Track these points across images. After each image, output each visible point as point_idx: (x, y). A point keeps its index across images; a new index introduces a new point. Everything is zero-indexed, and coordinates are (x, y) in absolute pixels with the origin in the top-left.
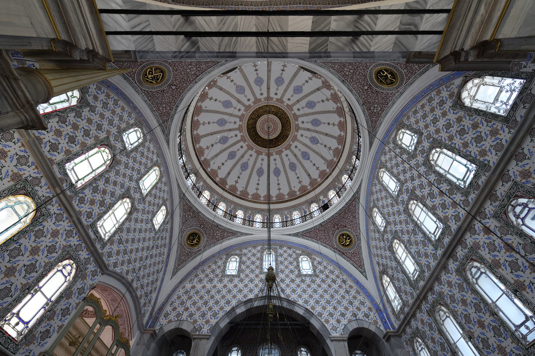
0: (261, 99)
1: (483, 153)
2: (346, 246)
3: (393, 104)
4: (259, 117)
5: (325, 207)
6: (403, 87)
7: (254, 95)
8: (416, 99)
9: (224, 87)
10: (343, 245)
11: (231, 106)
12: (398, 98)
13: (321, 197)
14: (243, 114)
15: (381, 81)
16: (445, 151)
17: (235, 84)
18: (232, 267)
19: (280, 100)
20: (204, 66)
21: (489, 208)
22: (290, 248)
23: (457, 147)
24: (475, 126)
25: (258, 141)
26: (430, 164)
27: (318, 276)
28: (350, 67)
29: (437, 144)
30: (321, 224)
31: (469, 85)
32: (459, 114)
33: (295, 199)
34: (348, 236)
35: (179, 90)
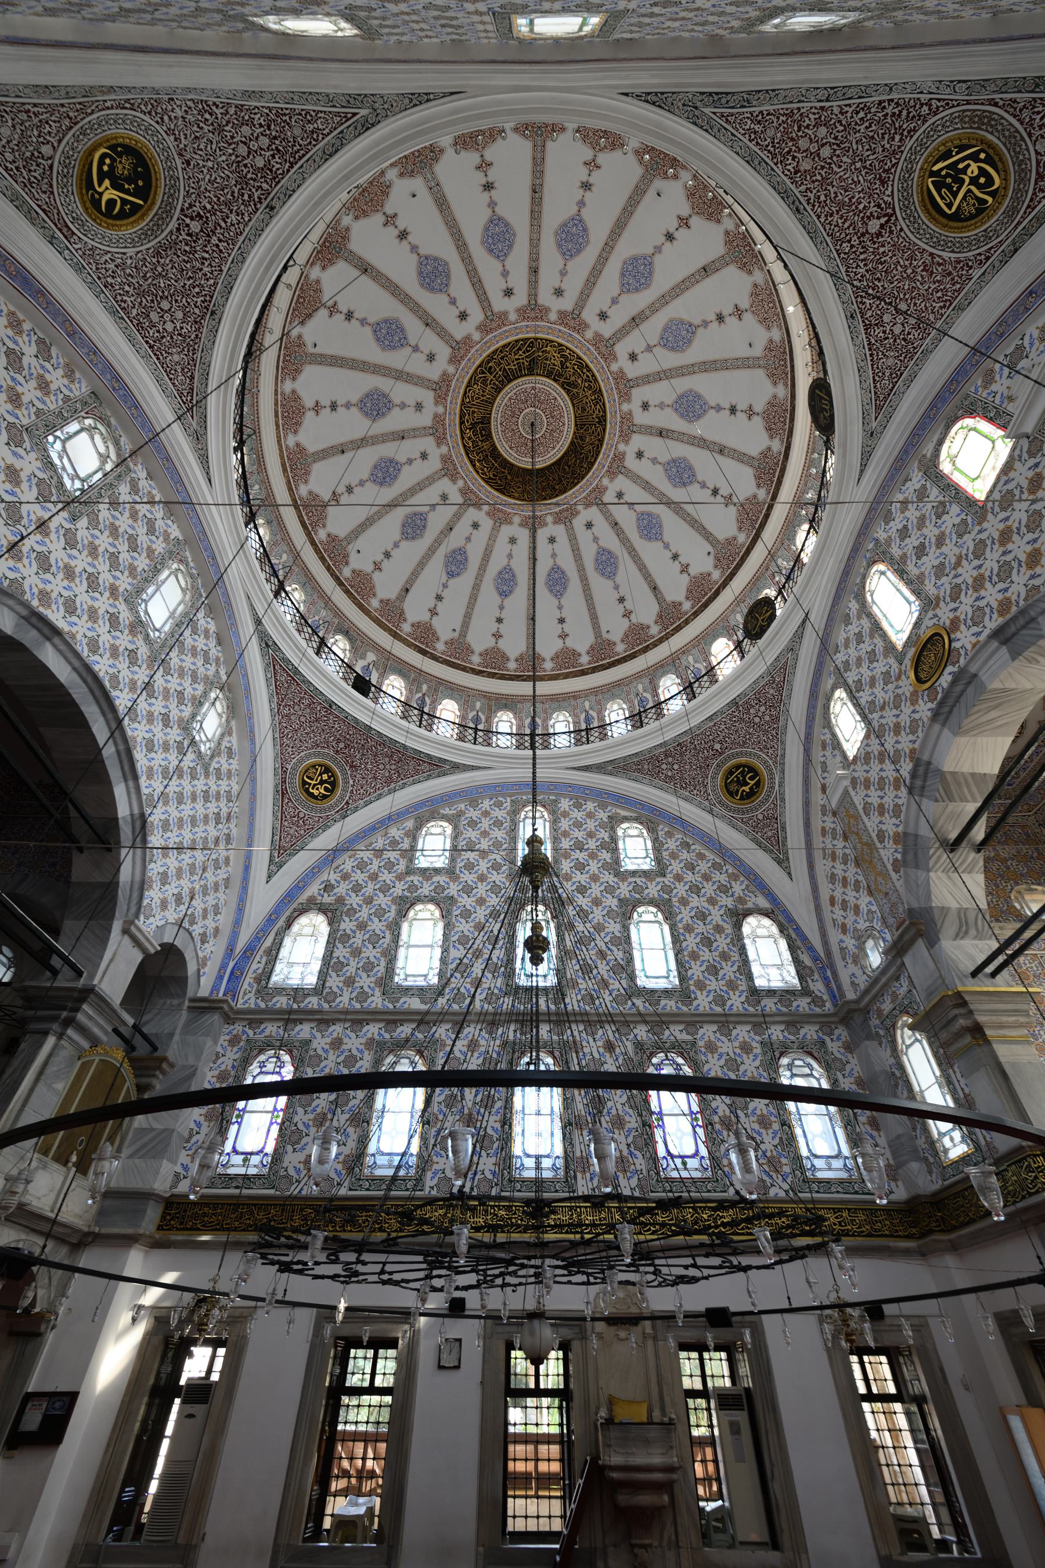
0: (629, 400)
1: (701, 985)
2: (307, 791)
3: (686, 799)
4: (568, 386)
5: (362, 685)
6: (725, 812)
7: (647, 379)
9: (709, 283)
10: (304, 783)
11: (626, 288)
12: (699, 805)
14: (587, 326)
15: (731, 773)
16: (666, 928)
17: (705, 324)
18: (83, 454)
19: (618, 467)
20: (890, 362)
22: (219, 643)
23: (684, 944)
24: (725, 956)
25: (485, 381)
26: (631, 914)
27: (207, 775)
28: (767, 718)
30: (331, 704)
31: (767, 922)
32: (725, 926)
33: (328, 568)
34: (334, 784)
35: (855, 241)
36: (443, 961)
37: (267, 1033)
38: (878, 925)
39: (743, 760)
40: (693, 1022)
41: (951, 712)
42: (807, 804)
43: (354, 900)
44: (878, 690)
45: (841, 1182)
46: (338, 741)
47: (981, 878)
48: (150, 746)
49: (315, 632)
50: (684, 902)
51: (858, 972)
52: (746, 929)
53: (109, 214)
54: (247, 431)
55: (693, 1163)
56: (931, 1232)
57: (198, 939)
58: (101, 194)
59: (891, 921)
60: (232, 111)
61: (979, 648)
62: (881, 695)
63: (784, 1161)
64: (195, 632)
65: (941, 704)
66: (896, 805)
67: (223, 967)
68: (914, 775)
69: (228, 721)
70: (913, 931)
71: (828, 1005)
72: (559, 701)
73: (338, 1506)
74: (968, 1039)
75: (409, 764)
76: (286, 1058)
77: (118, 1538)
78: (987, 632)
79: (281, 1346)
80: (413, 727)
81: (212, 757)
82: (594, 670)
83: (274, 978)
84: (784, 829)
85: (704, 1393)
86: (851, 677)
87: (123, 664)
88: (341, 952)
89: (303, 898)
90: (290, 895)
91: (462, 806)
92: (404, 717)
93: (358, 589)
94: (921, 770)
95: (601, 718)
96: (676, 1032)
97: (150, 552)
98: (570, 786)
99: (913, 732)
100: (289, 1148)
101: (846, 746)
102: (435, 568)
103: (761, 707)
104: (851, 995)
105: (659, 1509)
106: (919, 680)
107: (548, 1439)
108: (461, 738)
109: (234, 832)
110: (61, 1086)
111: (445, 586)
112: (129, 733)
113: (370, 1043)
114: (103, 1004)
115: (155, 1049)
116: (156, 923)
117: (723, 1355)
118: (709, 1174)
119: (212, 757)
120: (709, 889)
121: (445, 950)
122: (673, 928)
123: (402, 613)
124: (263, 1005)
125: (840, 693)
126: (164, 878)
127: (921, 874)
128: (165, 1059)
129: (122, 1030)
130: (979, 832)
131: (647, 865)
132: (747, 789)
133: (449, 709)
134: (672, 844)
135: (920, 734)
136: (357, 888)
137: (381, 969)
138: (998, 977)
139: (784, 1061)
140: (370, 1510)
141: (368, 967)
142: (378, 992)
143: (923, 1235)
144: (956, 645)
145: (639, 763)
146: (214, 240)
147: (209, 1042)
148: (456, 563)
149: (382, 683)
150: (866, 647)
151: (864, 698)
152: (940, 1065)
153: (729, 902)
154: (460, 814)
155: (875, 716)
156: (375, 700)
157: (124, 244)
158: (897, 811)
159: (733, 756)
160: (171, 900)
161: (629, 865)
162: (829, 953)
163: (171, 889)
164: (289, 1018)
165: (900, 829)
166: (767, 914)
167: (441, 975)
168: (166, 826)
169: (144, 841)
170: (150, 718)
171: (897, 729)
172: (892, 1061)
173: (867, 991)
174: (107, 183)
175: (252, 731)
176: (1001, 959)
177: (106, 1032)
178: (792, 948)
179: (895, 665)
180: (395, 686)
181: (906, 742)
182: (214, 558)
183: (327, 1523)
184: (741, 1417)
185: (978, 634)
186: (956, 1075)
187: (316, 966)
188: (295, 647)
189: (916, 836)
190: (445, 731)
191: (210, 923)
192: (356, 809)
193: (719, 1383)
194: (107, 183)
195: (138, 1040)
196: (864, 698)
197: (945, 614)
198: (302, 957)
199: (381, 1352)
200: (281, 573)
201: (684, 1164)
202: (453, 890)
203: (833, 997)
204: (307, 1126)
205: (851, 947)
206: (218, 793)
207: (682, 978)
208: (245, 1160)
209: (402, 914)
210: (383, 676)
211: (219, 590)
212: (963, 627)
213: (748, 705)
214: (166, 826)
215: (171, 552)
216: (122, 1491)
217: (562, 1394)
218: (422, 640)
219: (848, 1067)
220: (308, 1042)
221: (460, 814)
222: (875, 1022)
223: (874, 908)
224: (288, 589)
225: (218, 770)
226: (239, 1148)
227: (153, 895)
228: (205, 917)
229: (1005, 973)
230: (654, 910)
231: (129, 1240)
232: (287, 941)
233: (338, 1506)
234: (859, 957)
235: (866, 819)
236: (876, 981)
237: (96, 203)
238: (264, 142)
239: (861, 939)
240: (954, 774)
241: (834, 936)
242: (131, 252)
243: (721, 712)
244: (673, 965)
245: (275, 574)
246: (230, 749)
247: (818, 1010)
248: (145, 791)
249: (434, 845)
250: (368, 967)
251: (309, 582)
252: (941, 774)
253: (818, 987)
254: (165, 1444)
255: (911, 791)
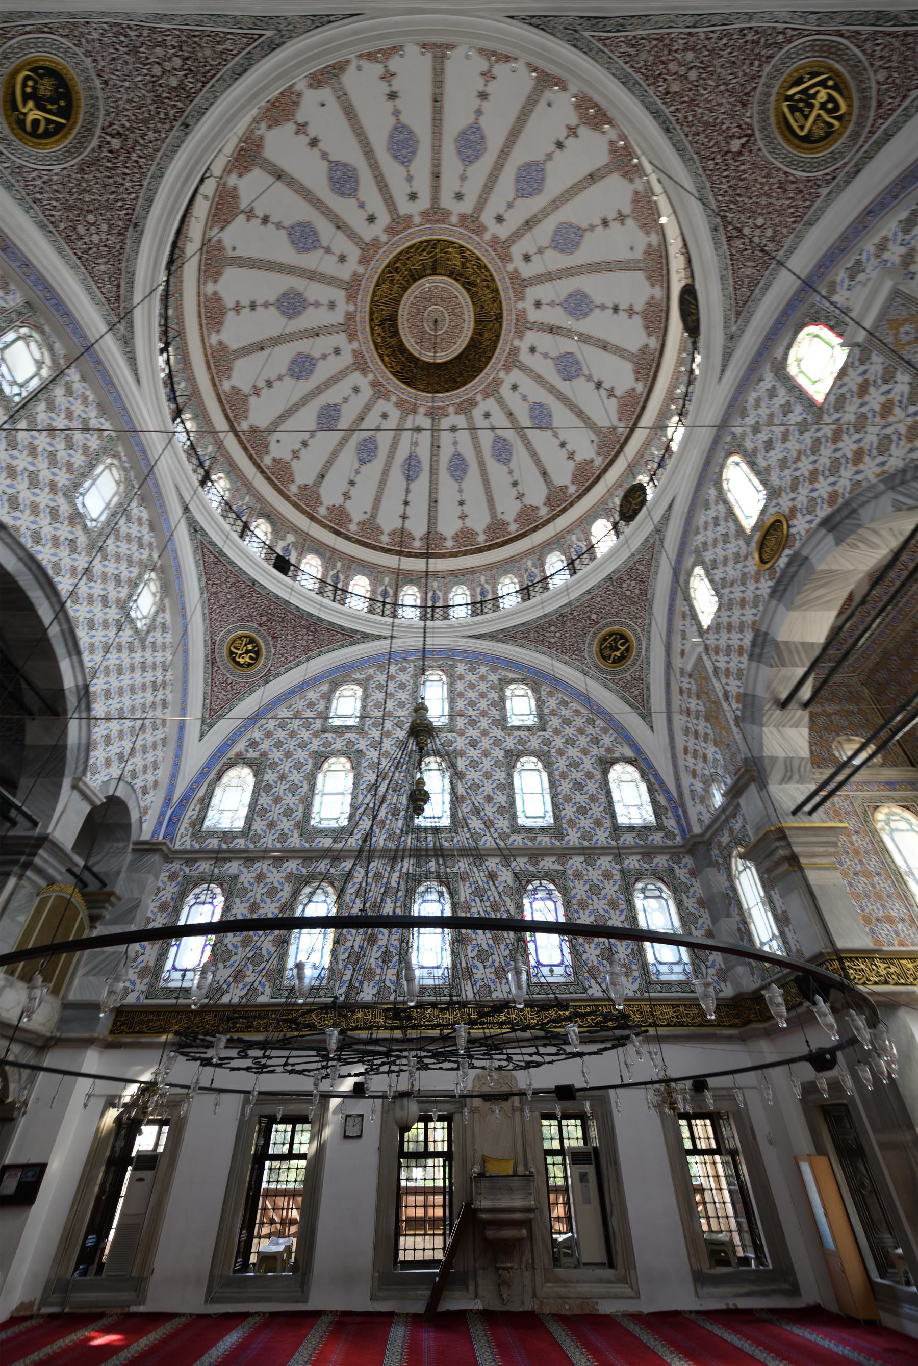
5: (282, 565)
6: (599, 674)
8: (586, 700)
13: (290, 538)
21: (521, 864)
27: (144, 648)
29: (545, 758)
30: (254, 582)
31: (630, 769)
33: (251, 457)
36: (354, 807)
37: (201, 869)
38: (720, 771)
39: (615, 628)
40: (564, 854)
41: (785, 590)
42: (669, 666)
43: (276, 755)
44: (729, 569)
45: (680, 983)
46: (261, 615)
47: (805, 731)
48: (91, 625)
49: (238, 517)
50: (561, 752)
51: (704, 811)
52: (612, 775)
53: (34, 134)
54: (171, 334)
55: (559, 971)
56: (750, 1022)
57: (139, 791)
58: (25, 114)
59: (731, 767)
60: (145, 33)
61: (811, 534)
62: (732, 572)
63: (634, 967)
64: (129, 520)
65: (778, 583)
66: (740, 670)
67: (162, 814)
68: (754, 644)
69: (161, 600)
70: (747, 777)
71: (679, 838)
72: (458, 576)
73: (263, 1246)
74: (786, 866)
75: (322, 634)
76: (218, 890)
77: (84, 1273)
78: (818, 520)
79: (215, 1125)
80: (327, 602)
81: (148, 632)
82: (490, 548)
83: (207, 823)
84: (648, 688)
85: (561, 1152)
86: (708, 556)
87: (64, 552)
88: (265, 800)
89: (232, 753)
90: (220, 752)
91: (371, 671)
92: (321, 593)
93: (278, 475)
94: (760, 639)
95: (495, 591)
96: (548, 864)
97: (86, 448)
98: (466, 652)
99: (755, 606)
100: (221, 965)
101: (701, 617)
102: (348, 457)
103: (631, 582)
104: (697, 830)
105: (520, 1240)
106: (763, 561)
107: (434, 1191)
108: (371, 611)
109: (170, 697)
110: (23, 919)
111: (357, 472)
112: (72, 614)
113: (289, 877)
114: (56, 849)
115: (104, 885)
116: (100, 780)
117: (579, 1122)
118: (572, 979)
119: (148, 632)
120: (583, 741)
121: (354, 797)
122: (551, 775)
123: (318, 498)
124: (197, 846)
125: (699, 570)
126: (108, 740)
127: (756, 728)
128: (112, 893)
129: (75, 870)
130: (806, 693)
131: (531, 721)
132: (618, 653)
133: (360, 585)
134: (552, 703)
135: (761, 608)
136: (278, 745)
137: (299, 815)
138: (815, 815)
139: (639, 885)
140: (288, 1249)
141: (288, 812)
142: (296, 834)
143: (744, 1024)
144: (793, 531)
145: (526, 632)
146: (134, 157)
147: (151, 879)
148: (367, 451)
149: (300, 562)
150: (721, 530)
151: (718, 574)
152: (764, 887)
153: (602, 752)
154: (369, 678)
155: (726, 591)
156: (294, 578)
157: (48, 161)
158: (739, 675)
159: (607, 625)
160: (115, 759)
161: (514, 721)
162: (681, 795)
163: (114, 749)
164: (219, 856)
165: (741, 690)
166: (630, 762)
167: (351, 817)
168: (107, 694)
169: (89, 709)
170: (90, 599)
171: (743, 603)
172: (727, 884)
173: (709, 827)
174: (30, 104)
175: (183, 608)
176: (817, 799)
177: (60, 873)
178: (650, 791)
179: (744, 547)
180: (312, 565)
181: (749, 615)
182: (144, 452)
183: (253, 1259)
184: (590, 1169)
185: (810, 522)
186: (776, 897)
187: (244, 812)
188: (222, 533)
189: (754, 696)
190: (357, 604)
191: (150, 777)
192: (278, 675)
193: (574, 1143)
194: (30, 104)
195: (87, 877)
196: (718, 574)
197: (785, 503)
198: (230, 805)
199: (299, 1127)
200: (207, 464)
201: (552, 971)
202: (362, 745)
203: (683, 831)
204: (236, 947)
205: (699, 790)
206: (154, 664)
207: (556, 817)
208: (184, 976)
209: (318, 767)
210: (301, 555)
211: (150, 482)
212: (799, 516)
213: (621, 581)
214: (107, 694)
215: (105, 448)
216: (86, 1238)
217: (446, 1156)
218: (337, 522)
219: (692, 890)
220: (235, 877)
221: (369, 678)
222: (715, 852)
223: (719, 757)
224: (214, 477)
225: (154, 643)
226: (178, 966)
227: (98, 755)
228: (145, 772)
229: (821, 810)
230: (535, 759)
231: (87, 1043)
232: (218, 791)
233: (263, 1246)
234: (705, 798)
235: (714, 681)
236: (717, 818)
237: (21, 123)
238: (177, 62)
239: (707, 782)
240: (786, 643)
241: (686, 780)
242: (56, 168)
243: (597, 586)
244: (549, 807)
245: (201, 465)
246: (164, 624)
247: (670, 843)
248: (87, 664)
249: (347, 705)
250: (288, 812)
251: (233, 471)
252: (776, 644)
253: (670, 823)
254: (121, 1201)
255: (751, 657)
